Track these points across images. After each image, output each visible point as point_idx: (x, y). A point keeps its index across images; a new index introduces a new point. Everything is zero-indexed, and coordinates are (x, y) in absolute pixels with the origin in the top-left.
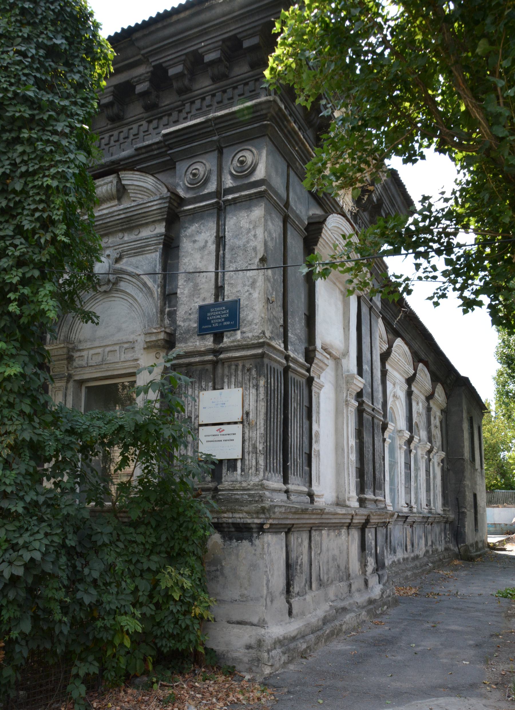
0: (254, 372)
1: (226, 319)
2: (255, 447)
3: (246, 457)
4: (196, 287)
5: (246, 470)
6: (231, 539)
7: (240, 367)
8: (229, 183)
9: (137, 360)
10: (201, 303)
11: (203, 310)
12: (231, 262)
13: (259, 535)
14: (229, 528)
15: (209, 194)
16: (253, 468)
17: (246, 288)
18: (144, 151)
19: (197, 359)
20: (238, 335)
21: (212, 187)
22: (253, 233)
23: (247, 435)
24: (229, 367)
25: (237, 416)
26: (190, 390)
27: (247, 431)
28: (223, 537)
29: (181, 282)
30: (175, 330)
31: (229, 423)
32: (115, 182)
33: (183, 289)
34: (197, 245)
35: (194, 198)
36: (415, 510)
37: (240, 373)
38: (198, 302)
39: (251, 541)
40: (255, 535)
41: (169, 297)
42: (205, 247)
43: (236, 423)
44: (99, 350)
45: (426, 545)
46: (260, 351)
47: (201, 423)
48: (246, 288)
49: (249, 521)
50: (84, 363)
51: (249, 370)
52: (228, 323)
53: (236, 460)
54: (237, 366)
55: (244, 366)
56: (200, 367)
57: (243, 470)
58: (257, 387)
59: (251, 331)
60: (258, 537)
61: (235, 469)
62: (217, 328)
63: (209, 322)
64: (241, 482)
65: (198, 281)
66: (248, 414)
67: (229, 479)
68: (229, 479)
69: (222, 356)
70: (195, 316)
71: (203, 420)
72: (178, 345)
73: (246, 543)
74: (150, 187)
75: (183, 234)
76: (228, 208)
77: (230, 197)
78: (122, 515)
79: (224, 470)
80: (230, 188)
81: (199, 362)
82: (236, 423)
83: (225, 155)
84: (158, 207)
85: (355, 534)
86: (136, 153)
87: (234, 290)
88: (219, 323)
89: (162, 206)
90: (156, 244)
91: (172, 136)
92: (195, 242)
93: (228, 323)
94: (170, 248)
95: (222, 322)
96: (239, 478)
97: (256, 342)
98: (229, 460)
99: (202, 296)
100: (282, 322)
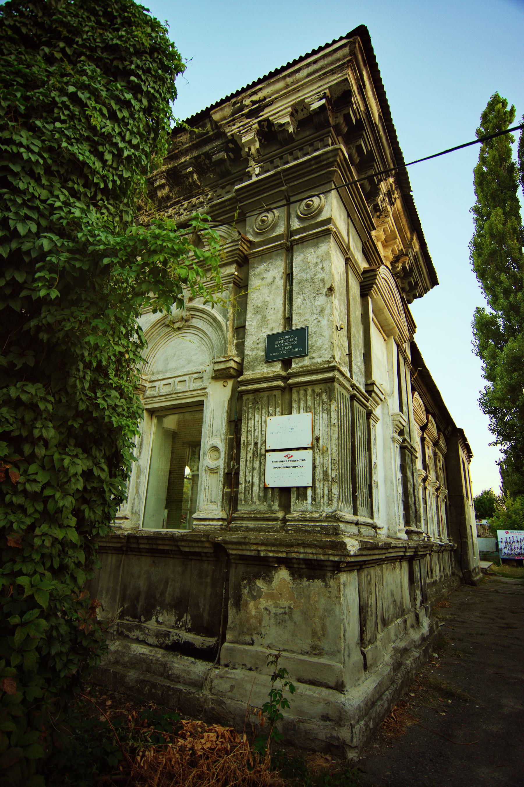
0: (324, 396)
1: (295, 346)
2: (326, 473)
3: (317, 485)
4: (264, 319)
5: (317, 500)
6: (301, 577)
7: (309, 392)
8: (296, 225)
10: (269, 333)
11: (271, 339)
12: (299, 294)
13: (334, 574)
14: (299, 564)
15: (277, 236)
16: (325, 497)
17: (315, 316)
18: (217, 207)
19: (265, 385)
20: (306, 361)
21: (281, 230)
22: (320, 266)
23: (317, 462)
24: (298, 392)
25: (307, 441)
26: (257, 416)
27: (317, 457)
28: (292, 574)
29: (249, 315)
30: (243, 360)
31: (298, 449)
33: (252, 322)
34: (266, 283)
35: (263, 241)
36: (432, 539)
37: (309, 398)
39: (324, 581)
40: (329, 574)
42: (273, 282)
43: (305, 449)
45: (440, 571)
46: (331, 375)
47: (267, 448)
48: (315, 316)
49: (322, 558)
51: (319, 395)
52: (297, 350)
53: (306, 488)
54: (306, 391)
55: (313, 391)
56: (266, 394)
57: (314, 499)
58: (329, 412)
59: (321, 357)
60: (333, 577)
62: (284, 355)
63: (277, 350)
64: (312, 513)
66: (317, 439)
67: (298, 509)
68: (299, 508)
69: (290, 381)
70: (262, 345)
71: (270, 445)
72: (245, 373)
73: (319, 583)
75: (252, 273)
76: (295, 247)
78: (183, 544)
79: (293, 499)
80: (298, 229)
81: (266, 388)
82: (305, 449)
85: (405, 565)
86: (211, 210)
87: (302, 319)
88: (287, 350)
91: (243, 191)
92: (263, 279)
93: (297, 350)
94: (241, 286)
95: (290, 349)
96: (309, 508)
97: (326, 366)
98: (298, 488)
99: (270, 326)
100: (347, 352)
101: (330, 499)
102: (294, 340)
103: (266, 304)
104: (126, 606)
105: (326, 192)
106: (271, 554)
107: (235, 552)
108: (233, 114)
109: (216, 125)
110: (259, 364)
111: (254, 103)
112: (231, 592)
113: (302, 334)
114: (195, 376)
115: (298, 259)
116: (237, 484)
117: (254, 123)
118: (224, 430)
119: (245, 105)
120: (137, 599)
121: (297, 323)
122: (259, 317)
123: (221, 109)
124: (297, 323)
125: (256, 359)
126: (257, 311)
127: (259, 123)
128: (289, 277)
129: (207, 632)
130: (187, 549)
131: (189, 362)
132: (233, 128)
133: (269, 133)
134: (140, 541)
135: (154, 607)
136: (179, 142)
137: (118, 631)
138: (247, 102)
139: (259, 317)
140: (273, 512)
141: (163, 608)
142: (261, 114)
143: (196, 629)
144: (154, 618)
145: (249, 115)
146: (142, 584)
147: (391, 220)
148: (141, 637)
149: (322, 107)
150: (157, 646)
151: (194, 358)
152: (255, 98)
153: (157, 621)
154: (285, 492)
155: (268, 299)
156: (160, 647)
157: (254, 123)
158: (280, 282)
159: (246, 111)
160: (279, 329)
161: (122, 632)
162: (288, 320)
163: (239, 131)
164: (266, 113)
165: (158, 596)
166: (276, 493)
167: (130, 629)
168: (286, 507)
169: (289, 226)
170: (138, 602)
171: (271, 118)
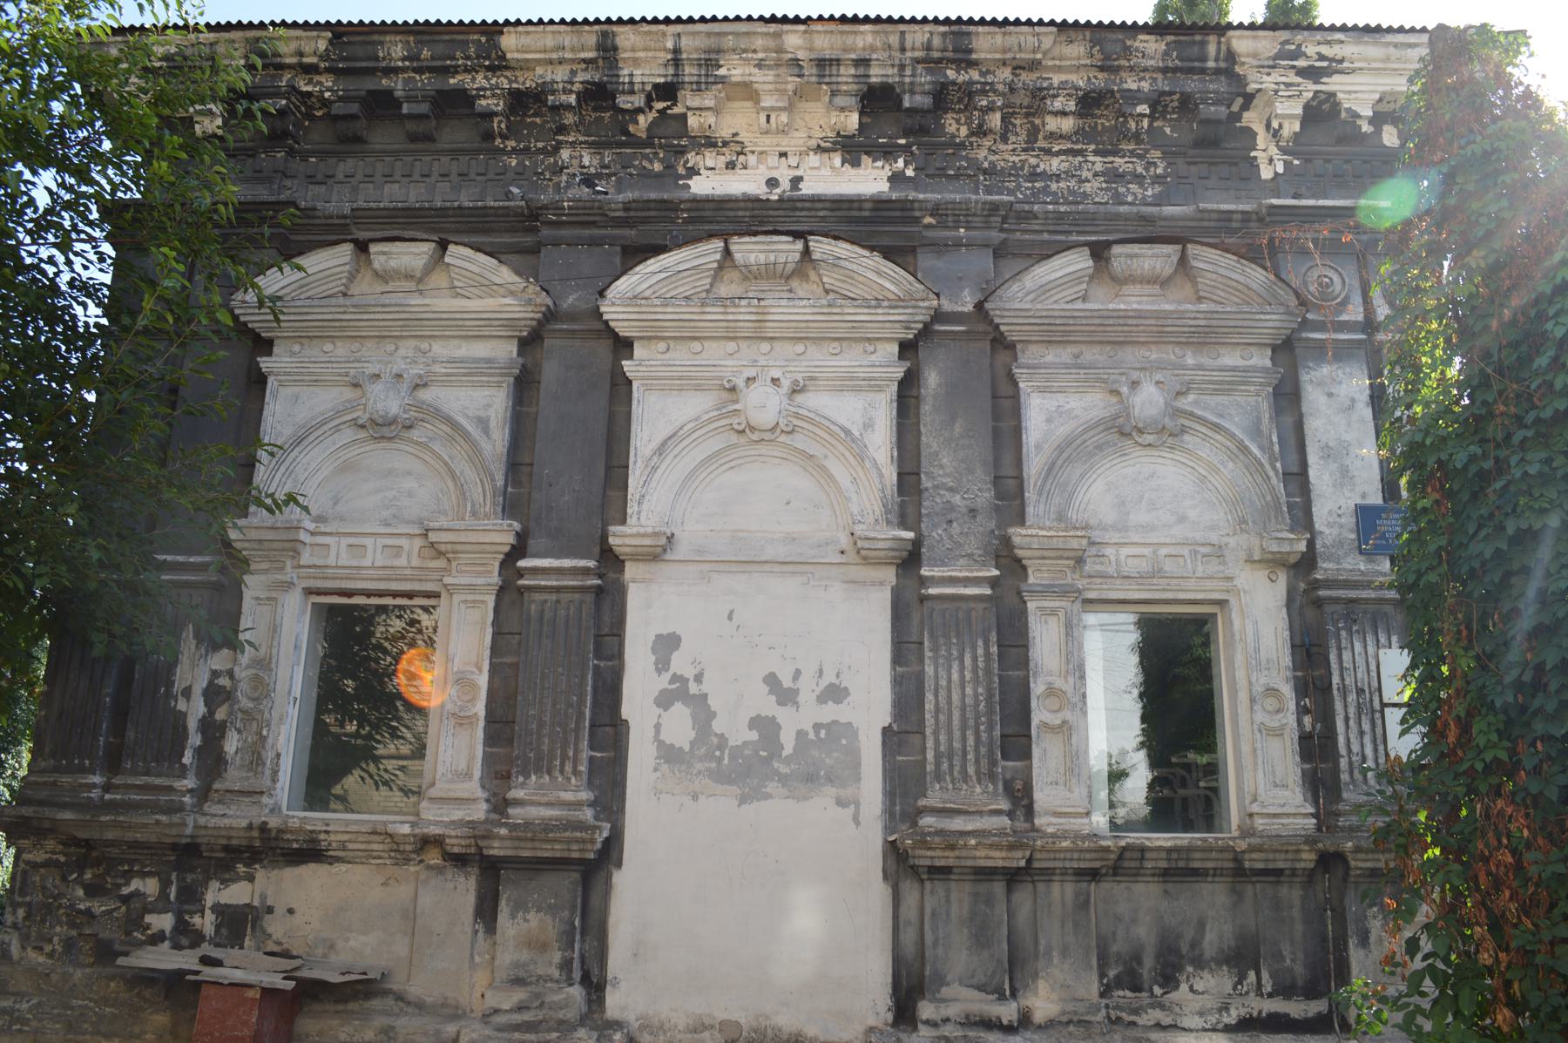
4: (1345, 475)
9: (1230, 579)
10: (1359, 501)
18: (1214, 216)
21: (1354, 313)
32: (1175, 259)
33: (1319, 474)
38: (1349, 501)
41: (1298, 479)
44: (1146, 551)
50: (1111, 570)
56: (1371, 607)
65: (1347, 462)
70: (1349, 521)
72: (1322, 564)
74: (1254, 286)
78: (1254, 856)
84: (1277, 324)
86: (1200, 215)
89: (1285, 325)
90: (1261, 384)
94: (1287, 397)
103: (1346, 447)
104: (1112, 973)
108: (1277, 57)
109: (1231, 57)
110: (1346, 555)
111: (1322, 57)
112: (1351, 928)
114: (1203, 550)
117: (1309, 88)
118: (1287, 660)
119: (1305, 54)
120: (1137, 958)
122: (1334, 466)
123: (1255, 38)
125: (1341, 543)
126: (1328, 453)
127: (1316, 92)
129: (1311, 993)
130: (1260, 865)
131: (1182, 519)
132: (1265, 78)
133: (1321, 113)
134: (1148, 855)
135: (1181, 969)
136: (1137, 50)
137: (1109, 1018)
138: (1311, 50)
139: (1334, 466)
141: (1199, 963)
142: (1324, 80)
143: (1284, 990)
144: (1184, 987)
145: (1301, 72)
146: (1145, 932)
148: (1167, 1021)
150: (1205, 1030)
151: (1192, 514)
152: (1325, 50)
153: (1191, 989)
155: (1347, 437)
156: (1214, 1030)
157: (1309, 88)
159: (1301, 63)
160: (1376, 499)
161: (1118, 1018)
163: (1276, 92)
164: (1334, 84)
165: (1184, 949)
167: (1136, 1012)
170: (1140, 963)
171: (1340, 95)
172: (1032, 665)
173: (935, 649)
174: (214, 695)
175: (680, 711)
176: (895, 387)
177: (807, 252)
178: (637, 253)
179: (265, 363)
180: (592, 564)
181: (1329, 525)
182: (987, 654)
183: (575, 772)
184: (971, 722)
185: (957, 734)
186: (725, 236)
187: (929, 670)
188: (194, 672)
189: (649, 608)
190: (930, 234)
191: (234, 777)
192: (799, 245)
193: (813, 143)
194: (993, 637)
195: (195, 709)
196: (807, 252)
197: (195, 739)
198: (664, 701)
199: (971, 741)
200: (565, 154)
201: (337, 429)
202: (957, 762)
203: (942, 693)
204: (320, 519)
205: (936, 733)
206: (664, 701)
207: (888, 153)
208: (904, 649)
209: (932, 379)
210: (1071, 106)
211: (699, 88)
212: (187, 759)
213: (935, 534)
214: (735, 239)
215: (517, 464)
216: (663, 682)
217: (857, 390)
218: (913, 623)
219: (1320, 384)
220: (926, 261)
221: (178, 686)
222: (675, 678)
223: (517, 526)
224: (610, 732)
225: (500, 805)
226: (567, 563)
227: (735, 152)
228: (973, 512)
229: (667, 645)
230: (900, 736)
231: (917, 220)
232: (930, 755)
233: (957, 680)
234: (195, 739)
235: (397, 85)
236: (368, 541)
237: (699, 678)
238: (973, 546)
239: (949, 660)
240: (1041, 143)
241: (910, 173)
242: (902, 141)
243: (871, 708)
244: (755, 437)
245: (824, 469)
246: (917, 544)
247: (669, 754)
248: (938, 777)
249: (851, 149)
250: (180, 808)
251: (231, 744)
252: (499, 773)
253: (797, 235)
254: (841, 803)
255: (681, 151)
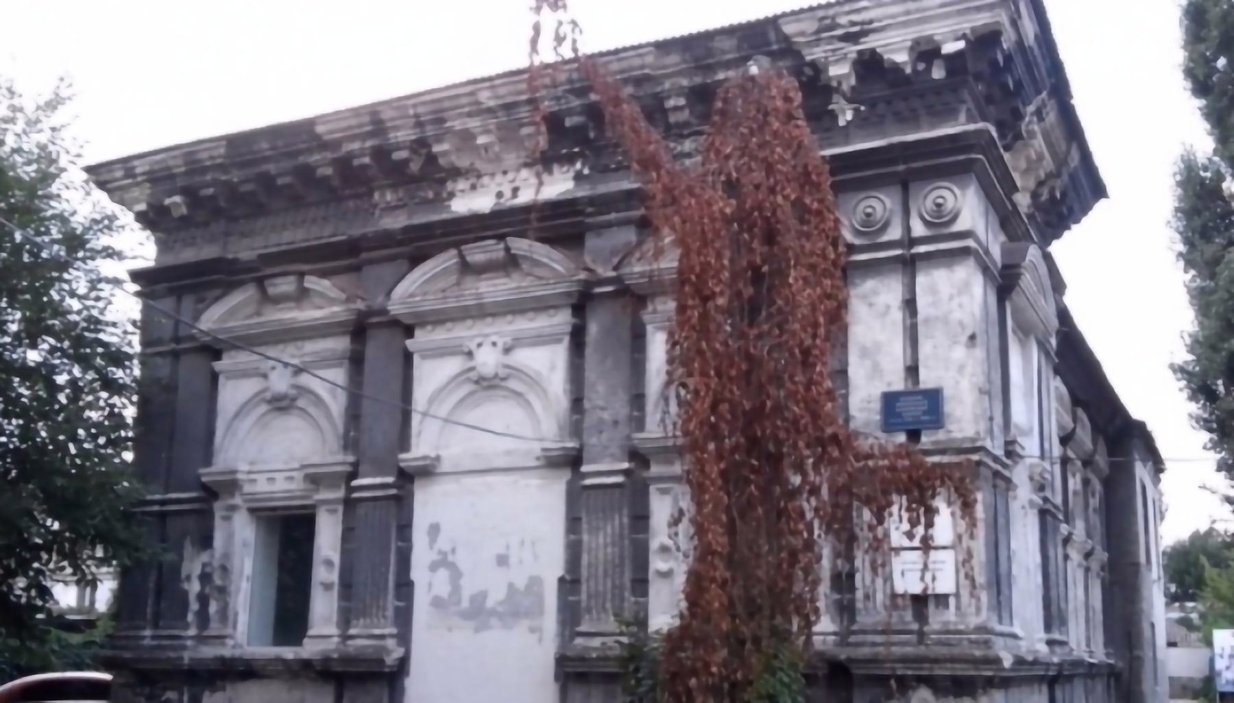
1: (925, 413)
8: (918, 229)
10: (886, 389)
11: (890, 400)
20: (941, 435)
21: (894, 233)
57: (958, 608)
60: (985, 692)
61: (947, 606)
63: (899, 415)
68: (937, 619)
70: (877, 405)
76: (918, 264)
77: (922, 249)
83: (912, 192)
101: (978, 610)
102: (924, 405)
103: (878, 346)
105: (963, 187)
106: (910, 672)
107: (863, 672)
109: (786, 39)
113: (934, 397)
115: (921, 280)
116: (852, 589)
121: (927, 379)
122: (868, 363)
124: (927, 379)
126: (864, 353)
127: (860, 53)
128: (910, 305)
139: (868, 363)
140: (908, 623)
142: (862, 40)
147: (1039, 142)
149: (959, 54)
154: (920, 602)
158: (897, 315)
160: (899, 385)
162: (912, 371)
163: (826, 58)
164: (869, 43)
166: (908, 602)
168: (921, 617)
169: (908, 229)
171: (878, 50)
172: (651, 531)
173: (589, 523)
174: (205, 578)
175: (443, 574)
176: (567, 339)
177: (507, 249)
178: (416, 260)
179: (218, 366)
180: (390, 480)
181: (861, 410)
182: (621, 524)
183: (384, 617)
184: (610, 572)
185: (601, 580)
186: (457, 245)
187: (585, 537)
188: (193, 566)
189: (429, 504)
190: (589, 220)
191: (214, 628)
192: (502, 246)
193: (522, 161)
194: (625, 511)
195: (194, 587)
196: (507, 249)
197: (194, 606)
198: (434, 567)
199: (609, 584)
200: (377, 196)
201: (257, 405)
202: (600, 601)
203: (593, 553)
204: (252, 463)
205: (588, 580)
206: (434, 567)
207: (570, 160)
208: (573, 523)
209: (593, 329)
210: (682, 101)
211: (439, 139)
212: (190, 617)
213: (592, 440)
214: (463, 247)
215: (354, 415)
216: (434, 556)
217: (544, 343)
218: (581, 505)
219: (864, 297)
220: (591, 242)
221: (183, 575)
222: (440, 552)
223: (351, 458)
224: (405, 587)
225: (345, 637)
226: (378, 480)
227: (474, 176)
228: (616, 423)
229: (434, 530)
230: (569, 584)
231: (581, 213)
232: (584, 596)
233: (601, 542)
234: (194, 606)
235: (271, 168)
236: (276, 475)
237: (453, 551)
238: (615, 450)
239: (598, 529)
240: (675, 131)
241: (586, 171)
242: (576, 150)
243: (552, 566)
244: (485, 384)
245: (528, 402)
246: (580, 451)
247: (437, 603)
248: (589, 610)
249: (545, 162)
250: (184, 648)
251: (213, 608)
252: (346, 619)
253: (501, 238)
254: (532, 630)
255: (442, 182)
